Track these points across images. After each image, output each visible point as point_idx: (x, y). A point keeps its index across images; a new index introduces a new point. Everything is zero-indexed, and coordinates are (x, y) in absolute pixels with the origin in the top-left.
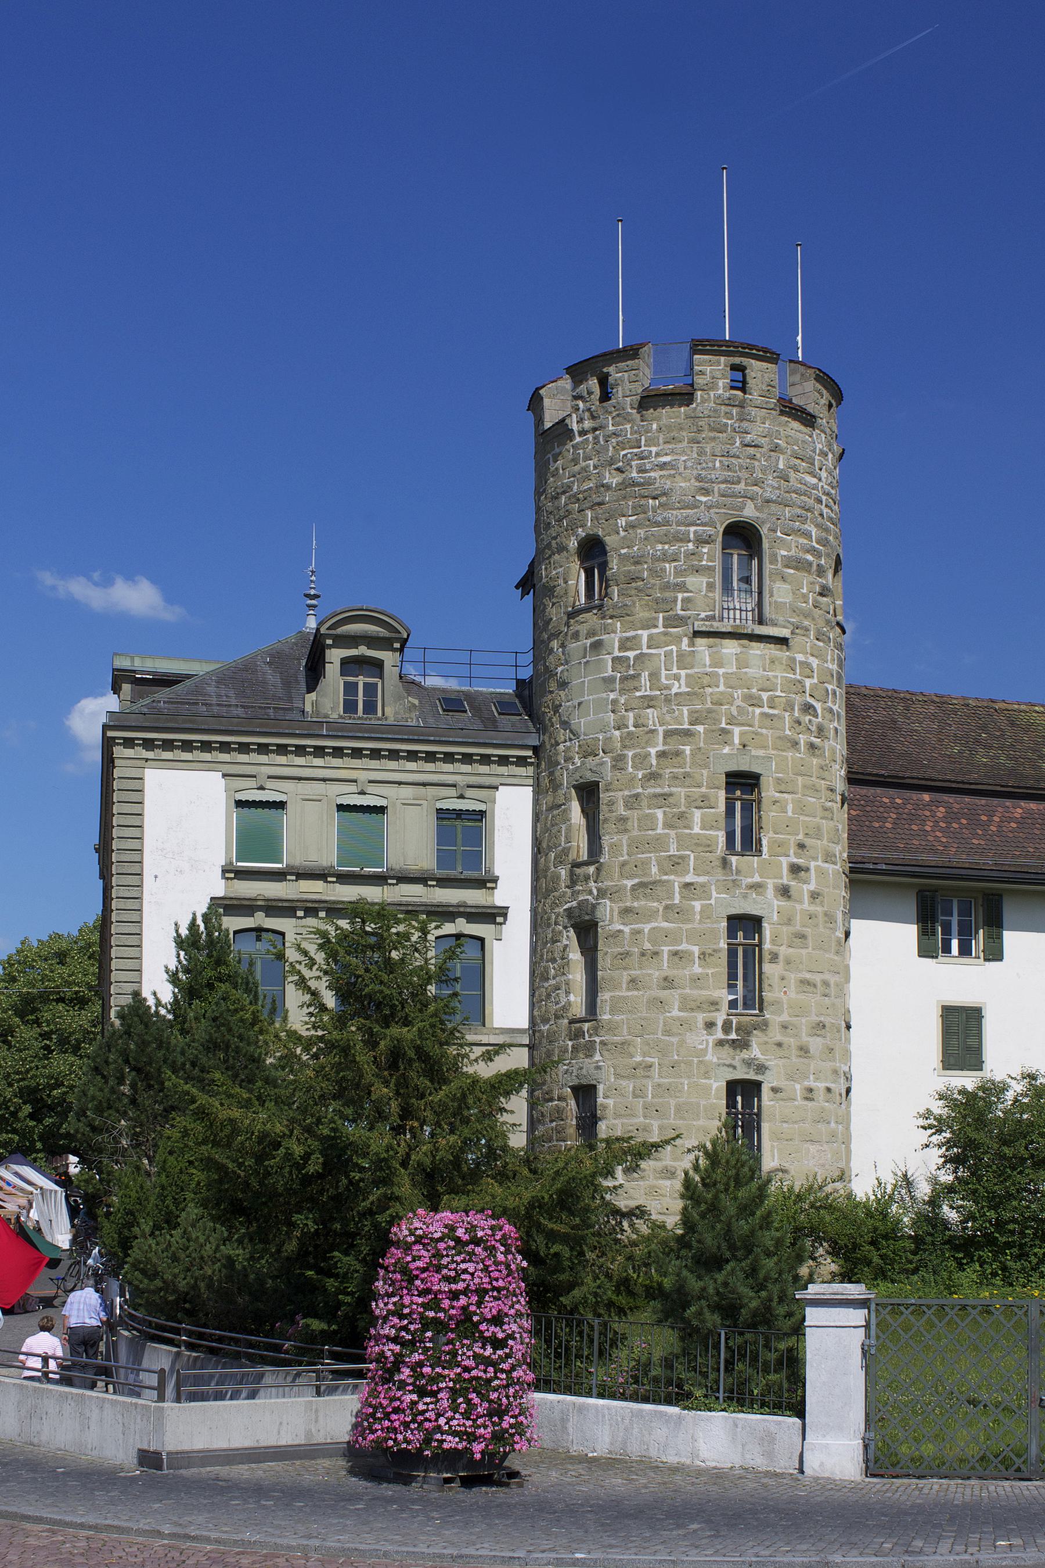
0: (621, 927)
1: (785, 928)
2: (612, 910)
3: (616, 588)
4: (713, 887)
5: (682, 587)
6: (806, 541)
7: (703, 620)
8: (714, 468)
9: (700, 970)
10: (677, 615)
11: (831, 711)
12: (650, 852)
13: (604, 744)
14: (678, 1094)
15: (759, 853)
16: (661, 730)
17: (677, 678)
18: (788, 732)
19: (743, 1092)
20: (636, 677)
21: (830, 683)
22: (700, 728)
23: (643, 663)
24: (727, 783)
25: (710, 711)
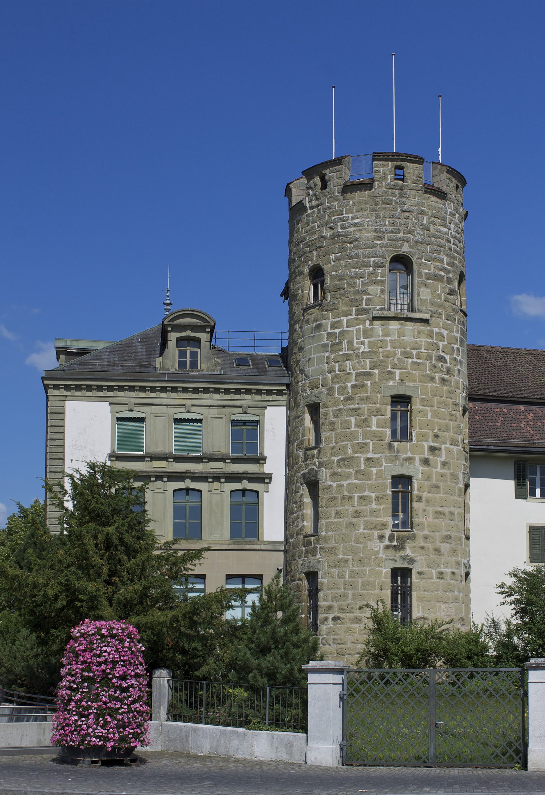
0: (332, 483)
1: (426, 483)
2: (326, 474)
3: (329, 294)
4: (383, 460)
5: (366, 292)
6: (440, 264)
7: (378, 310)
8: (385, 225)
9: (376, 507)
10: (363, 308)
11: (456, 360)
12: (348, 441)
13: (322, 381)
14: (363, 576)
15: (411, 440)
16: (354, 373)
17: (363, 343)
18: (428, 372)
19: (400, 575)
20: (340, 343)
21: (455, 344)
22: (376, 371)
23: (344, 335)
24: (392, 402)
25: (381, 361)
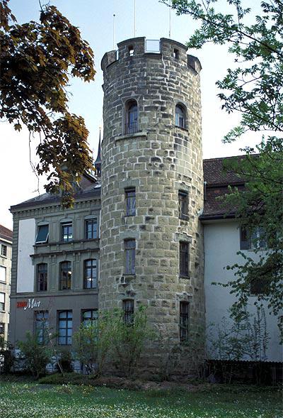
18: (146, 169)
22: (117, 174)
